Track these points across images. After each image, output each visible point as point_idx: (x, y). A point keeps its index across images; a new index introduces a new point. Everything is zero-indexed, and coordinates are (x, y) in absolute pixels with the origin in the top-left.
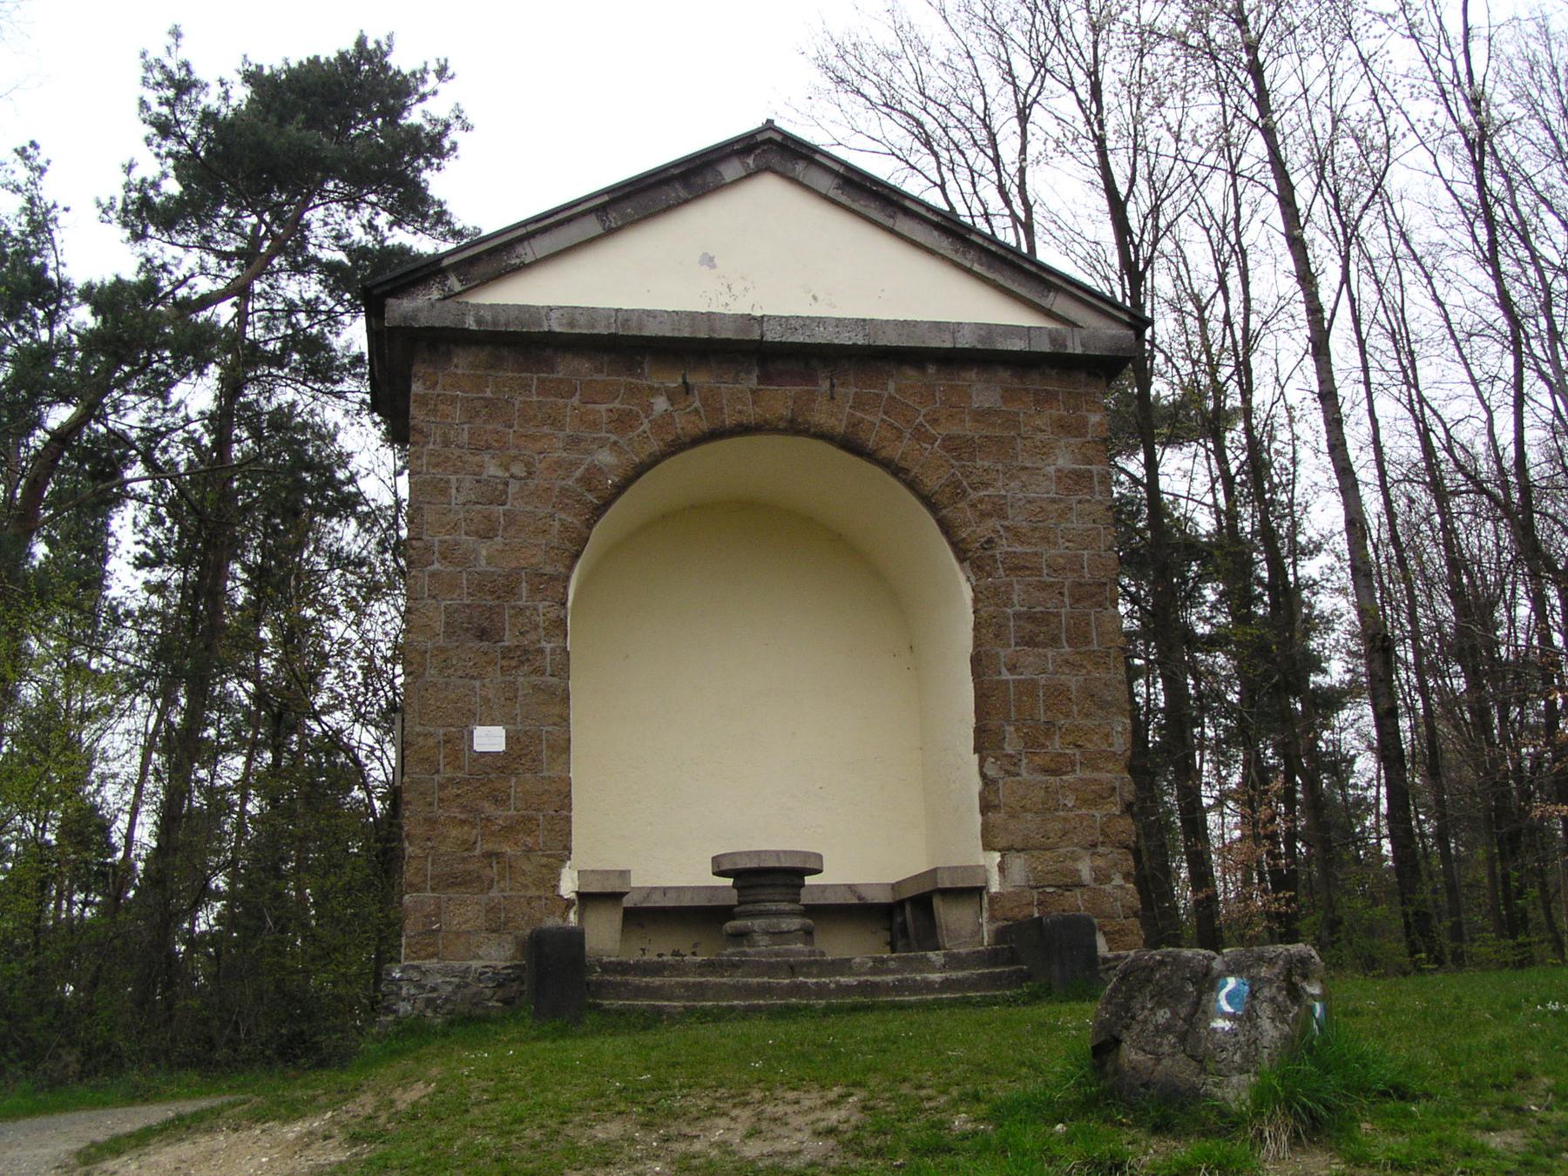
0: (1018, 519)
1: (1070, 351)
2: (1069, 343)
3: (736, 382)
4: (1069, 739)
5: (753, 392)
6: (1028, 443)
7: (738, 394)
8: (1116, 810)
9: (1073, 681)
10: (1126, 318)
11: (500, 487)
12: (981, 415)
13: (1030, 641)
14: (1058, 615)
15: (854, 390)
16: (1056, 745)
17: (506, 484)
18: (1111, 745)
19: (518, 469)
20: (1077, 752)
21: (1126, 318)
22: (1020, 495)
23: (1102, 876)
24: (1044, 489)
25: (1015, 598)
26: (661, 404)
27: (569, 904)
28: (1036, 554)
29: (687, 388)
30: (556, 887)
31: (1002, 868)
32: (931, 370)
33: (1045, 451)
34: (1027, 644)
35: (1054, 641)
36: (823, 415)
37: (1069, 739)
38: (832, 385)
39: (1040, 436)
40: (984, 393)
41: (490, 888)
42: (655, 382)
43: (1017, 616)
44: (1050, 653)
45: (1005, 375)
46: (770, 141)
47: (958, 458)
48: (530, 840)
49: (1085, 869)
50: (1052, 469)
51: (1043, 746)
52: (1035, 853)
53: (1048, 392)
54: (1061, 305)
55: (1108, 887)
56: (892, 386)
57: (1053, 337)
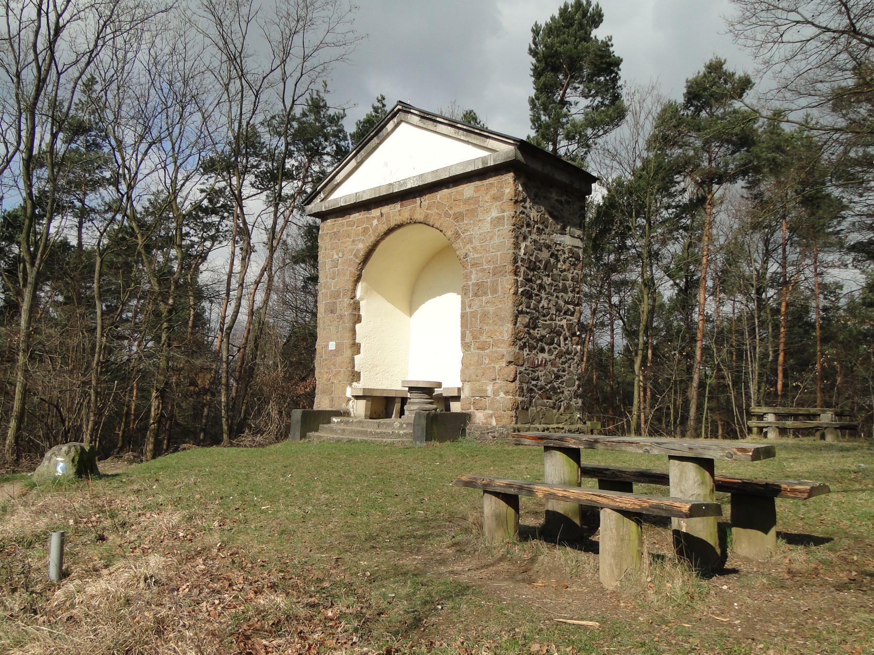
0: (476, 243)
7: (394, 212)
8: (504, 365)
9: (491, 309)
12: (467, 201)
13: (476, 295)
16: (484, 338)
19: (340, 255)
23: (496, 393)
24: (487, 227)
25: (473, 277)
26: (375, 222)
27: (349, 400)
33: (488, 211)
35: (485, 293)
36: (419, 216)
40: (468, 190)
44: (484, 298)
46: (399, 110)
47: (458, 222)
49: (490, 389)
54: (491, 143)
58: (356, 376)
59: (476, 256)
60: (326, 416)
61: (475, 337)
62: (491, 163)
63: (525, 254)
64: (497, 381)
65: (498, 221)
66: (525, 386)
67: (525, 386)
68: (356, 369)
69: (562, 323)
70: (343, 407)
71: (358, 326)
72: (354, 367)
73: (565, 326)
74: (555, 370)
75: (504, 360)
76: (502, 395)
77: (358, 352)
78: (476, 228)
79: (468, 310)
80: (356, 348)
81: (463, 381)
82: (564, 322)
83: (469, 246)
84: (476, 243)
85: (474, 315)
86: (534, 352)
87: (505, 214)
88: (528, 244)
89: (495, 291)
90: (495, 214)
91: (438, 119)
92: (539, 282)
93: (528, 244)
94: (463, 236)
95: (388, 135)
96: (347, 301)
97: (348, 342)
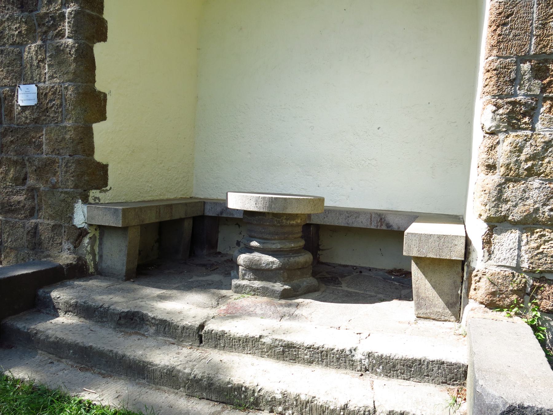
27: (82, 233)
30: (71, 218)
31: (487, 242)
48: (54, 179)
58: (98, 176)
71: (99, 49)
72: (90, 149)
80: (94, 105)
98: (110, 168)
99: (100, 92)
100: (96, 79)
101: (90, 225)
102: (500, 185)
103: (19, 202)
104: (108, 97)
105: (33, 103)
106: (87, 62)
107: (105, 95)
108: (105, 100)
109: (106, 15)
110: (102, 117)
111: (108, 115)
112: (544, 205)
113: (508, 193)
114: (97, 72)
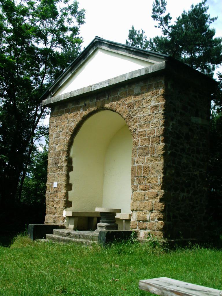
1: (149, 72)
2: (149, 70)
3: (93, 101)
4: (148, 181)
5: (96, 103)
6: (145, 100)
8: (158, 200)
10: (163, 58)
11: (59, 134)
14: (148, 147)
15: (112, 96)
16: (145, 182)
17: (60, 133)
18: (157, 182)
19: (61, 130)
20: (150, 184)
21: (163, 58)
22: (142, 115)
25: (139, 144)
28: (144, 131)
29: (85, 105)
32: (127, 87)
34: (141, 156)
37: (148, 181)
38: (108, 97)
39: (148, 97)
41: (55, 214)
42: (81, 105)
43: (139, 148)
45: (142, 84)
46: (96, 42)
50: (150, 106)
51: (142, 183)
52: (139, 211)
53: (151, 84)
55: (154, 222)
56: (119, 94)
57: (146, 70)
59: (141, 130)
60: (50, 229)
61: (140, 182)
62: (151, 71)
63: (172, 129)
64: (154, 211)
65: (156, 107)
66: (171, 214)
67: (171, 214)
68: (69, 200)
69: (196, 173)
70: (60, 223)
71: (71, 173)
73: (198, 175)
74: (191, 203)
75: (158, 197)
76: (156, 220)
77: (71, 189)
78: (142, 113)
79: (136, 165)
81: (132, 210)
82: (197, 173)
83: (137, 124)
84: (141, 122)
85: (140, 168)
86: (178, 192)
87: (159, 103)
88: (174, 122)
89: (153, 153)
90: (153, 104)
91: (119, 46)
92: (181, 147)
93: (174, 122)
94: (133, 117)
95: (90, 57)
96: (64, 157)
97: (64, 183)
98: (73, 202)
99: (70, 184)
100: (70, 180)
101: (66, 216)
102: (133, 203)
103: (52, 211)
104: (73, 184)
105: (56, 187)
106: (68, 177)
107: (72, 184)
108: (72, 185)
109: (73, 165)
110: (71, 189)
111: (72, 189)
112: (139, 206)
113: (134, 204)
114: (70, 179)
